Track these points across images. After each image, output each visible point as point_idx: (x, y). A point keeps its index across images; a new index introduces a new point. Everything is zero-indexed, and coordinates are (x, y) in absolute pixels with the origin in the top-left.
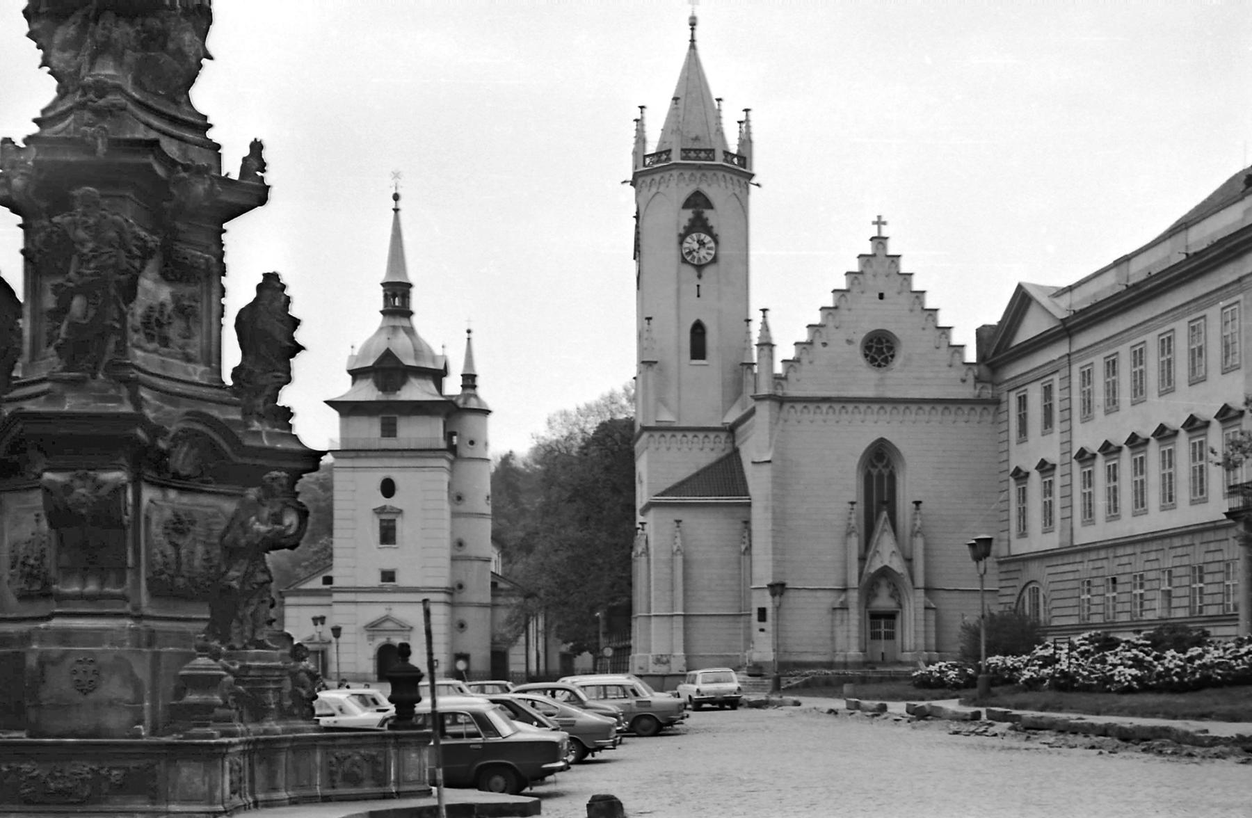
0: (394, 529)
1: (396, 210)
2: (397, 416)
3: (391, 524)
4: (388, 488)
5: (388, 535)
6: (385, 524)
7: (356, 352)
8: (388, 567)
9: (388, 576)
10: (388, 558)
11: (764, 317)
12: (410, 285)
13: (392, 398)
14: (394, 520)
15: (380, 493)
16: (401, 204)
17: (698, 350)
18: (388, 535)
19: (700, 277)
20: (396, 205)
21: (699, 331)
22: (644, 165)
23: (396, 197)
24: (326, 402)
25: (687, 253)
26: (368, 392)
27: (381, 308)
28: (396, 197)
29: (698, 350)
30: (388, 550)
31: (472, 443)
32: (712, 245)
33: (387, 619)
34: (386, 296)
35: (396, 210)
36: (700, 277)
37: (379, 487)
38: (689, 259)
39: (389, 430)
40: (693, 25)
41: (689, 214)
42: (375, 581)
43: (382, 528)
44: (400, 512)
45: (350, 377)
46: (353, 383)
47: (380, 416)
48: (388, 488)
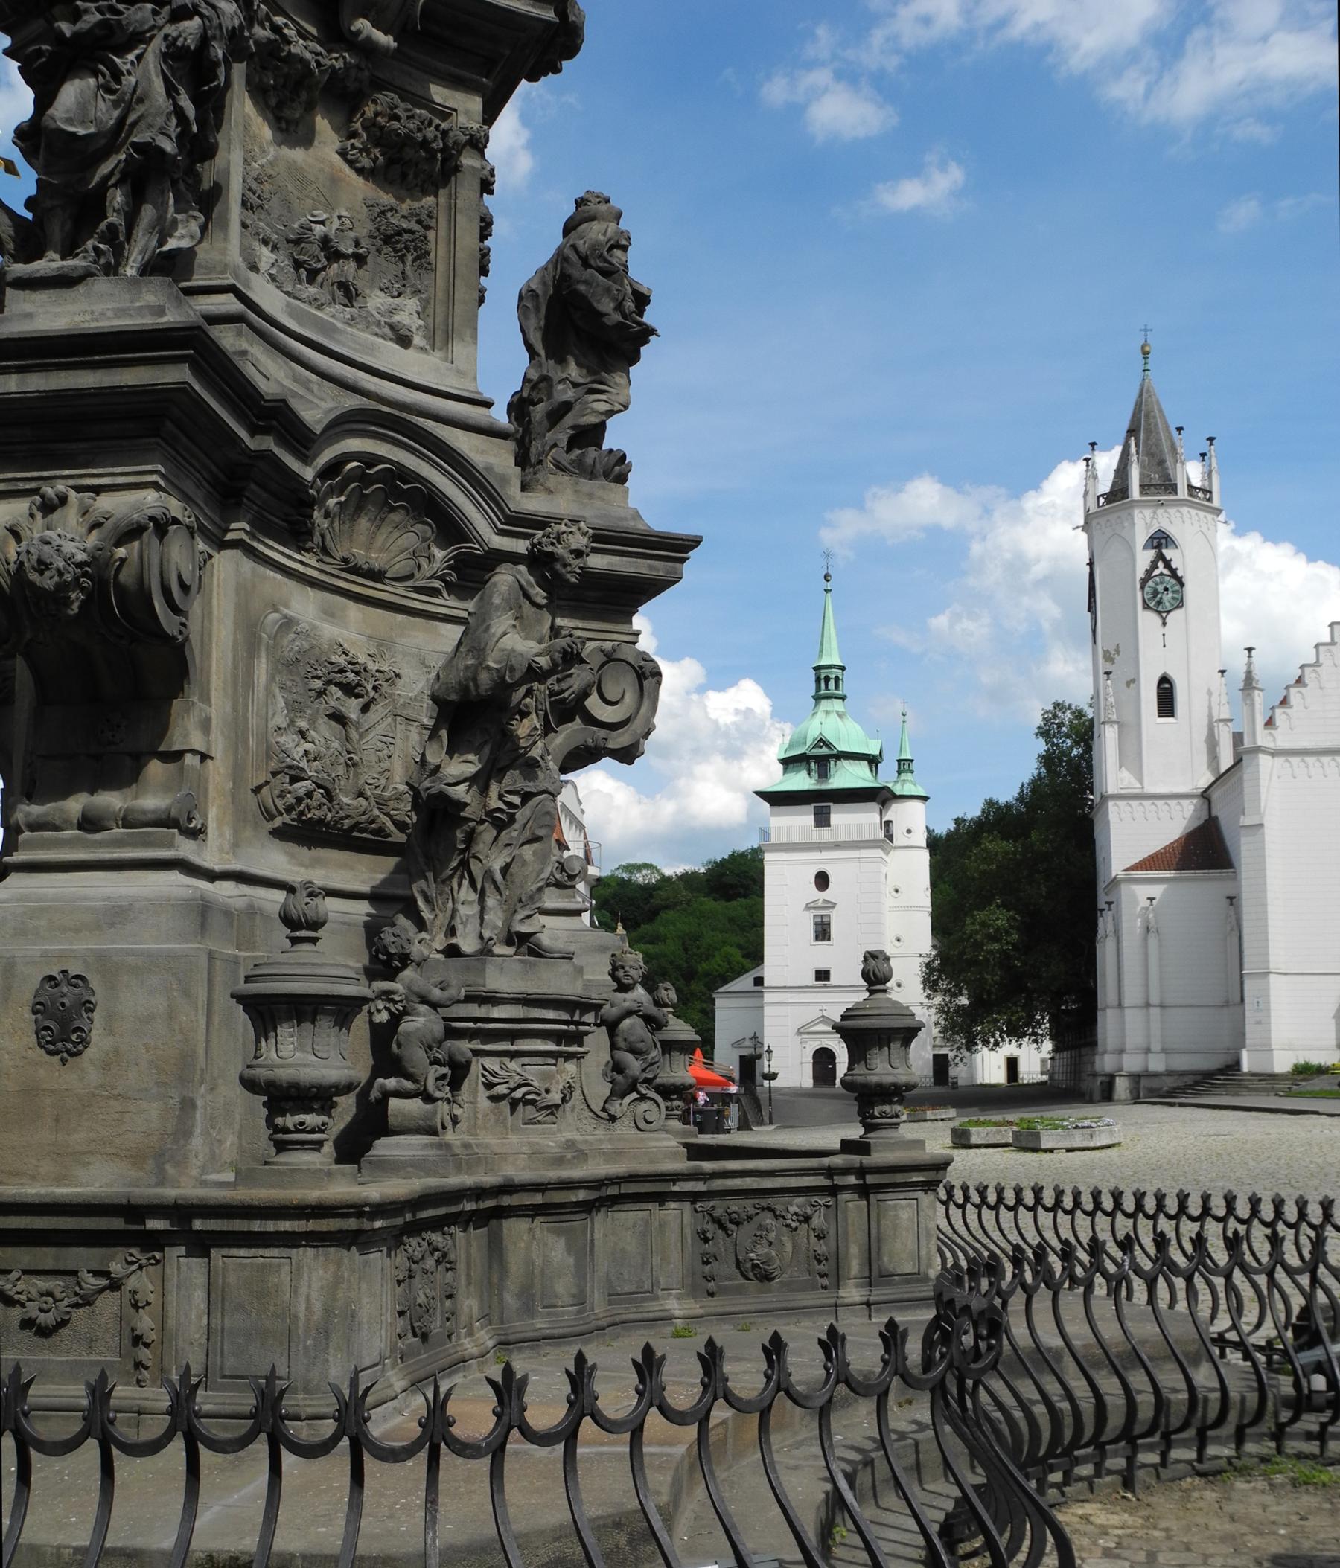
2: (831, 804)
4: (822, 880)
5: (822, 932)
6: (819, 919)
8: (822, 967)
9: (823, 975)
10: (823, 956)
11: (1250, 657)
13: (824, 787)
17: (1166, 704)
18: (822, 932)
19: (1164, 624)
21: (1167, 686)
22: (1099, 506)
23: (827, 577)
24: (756, 793)
25: (1149, 599)
26: (801, 781)
28: (827, 577)
29: (1166, 704)
31: (909, 831)
32: (1178, 587)
36: (1164, 624)
37: (813, 880)
38: (1152, 605)
39: (822, 819)
40: (1146, 354)
41: (1151, 554)
42: (810, 979)
43: (816, 924)
44: (834, 905)
45: (781, 766)
46: (785, 771)
47: (813, 805)
48: (822, 880)
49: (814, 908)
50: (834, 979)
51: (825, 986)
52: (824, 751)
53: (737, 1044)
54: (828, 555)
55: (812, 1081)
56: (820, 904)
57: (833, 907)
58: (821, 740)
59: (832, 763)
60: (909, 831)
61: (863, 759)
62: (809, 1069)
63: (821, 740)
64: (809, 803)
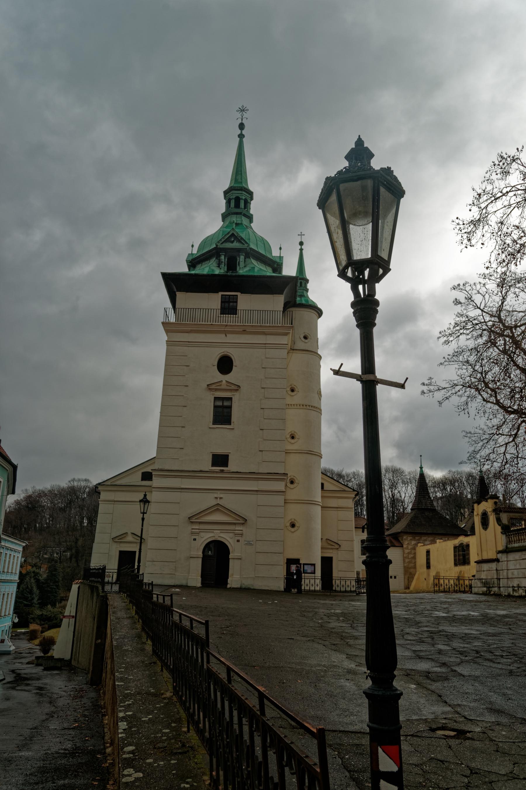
0: (230, 407)
1: (241, 136)
2: (238, 294)
3: (226, 403)
6: (219, 403)
7: (195, 251)
12: (251, 194)
14: (230, 399)
15: (216, 367)
16: (244, 132)
20: (241, 132)
23: (242, 126)
27: (223, 210)
28: (242, 126)
30: (222, 430)
33: (218, 508)
34: (228, 202)
35: (241, 136)
37: (216, 363)
42: (207, 464)
43: (215, 407)
47: (221, 293)
49: (216, 390)
50: (233, 466)
51: (222, 471)
52: (236, 245)
53: (118, 539)
54: (242, 110)
55: (199, 579)
56: (224, 385)
57: (237, 390)
58: (233, 235)
59: (242, 258)
60: (305, 338)
61: (269, 265)
62: (197, 565)
63: (233, 235)
64: (217, 292)
